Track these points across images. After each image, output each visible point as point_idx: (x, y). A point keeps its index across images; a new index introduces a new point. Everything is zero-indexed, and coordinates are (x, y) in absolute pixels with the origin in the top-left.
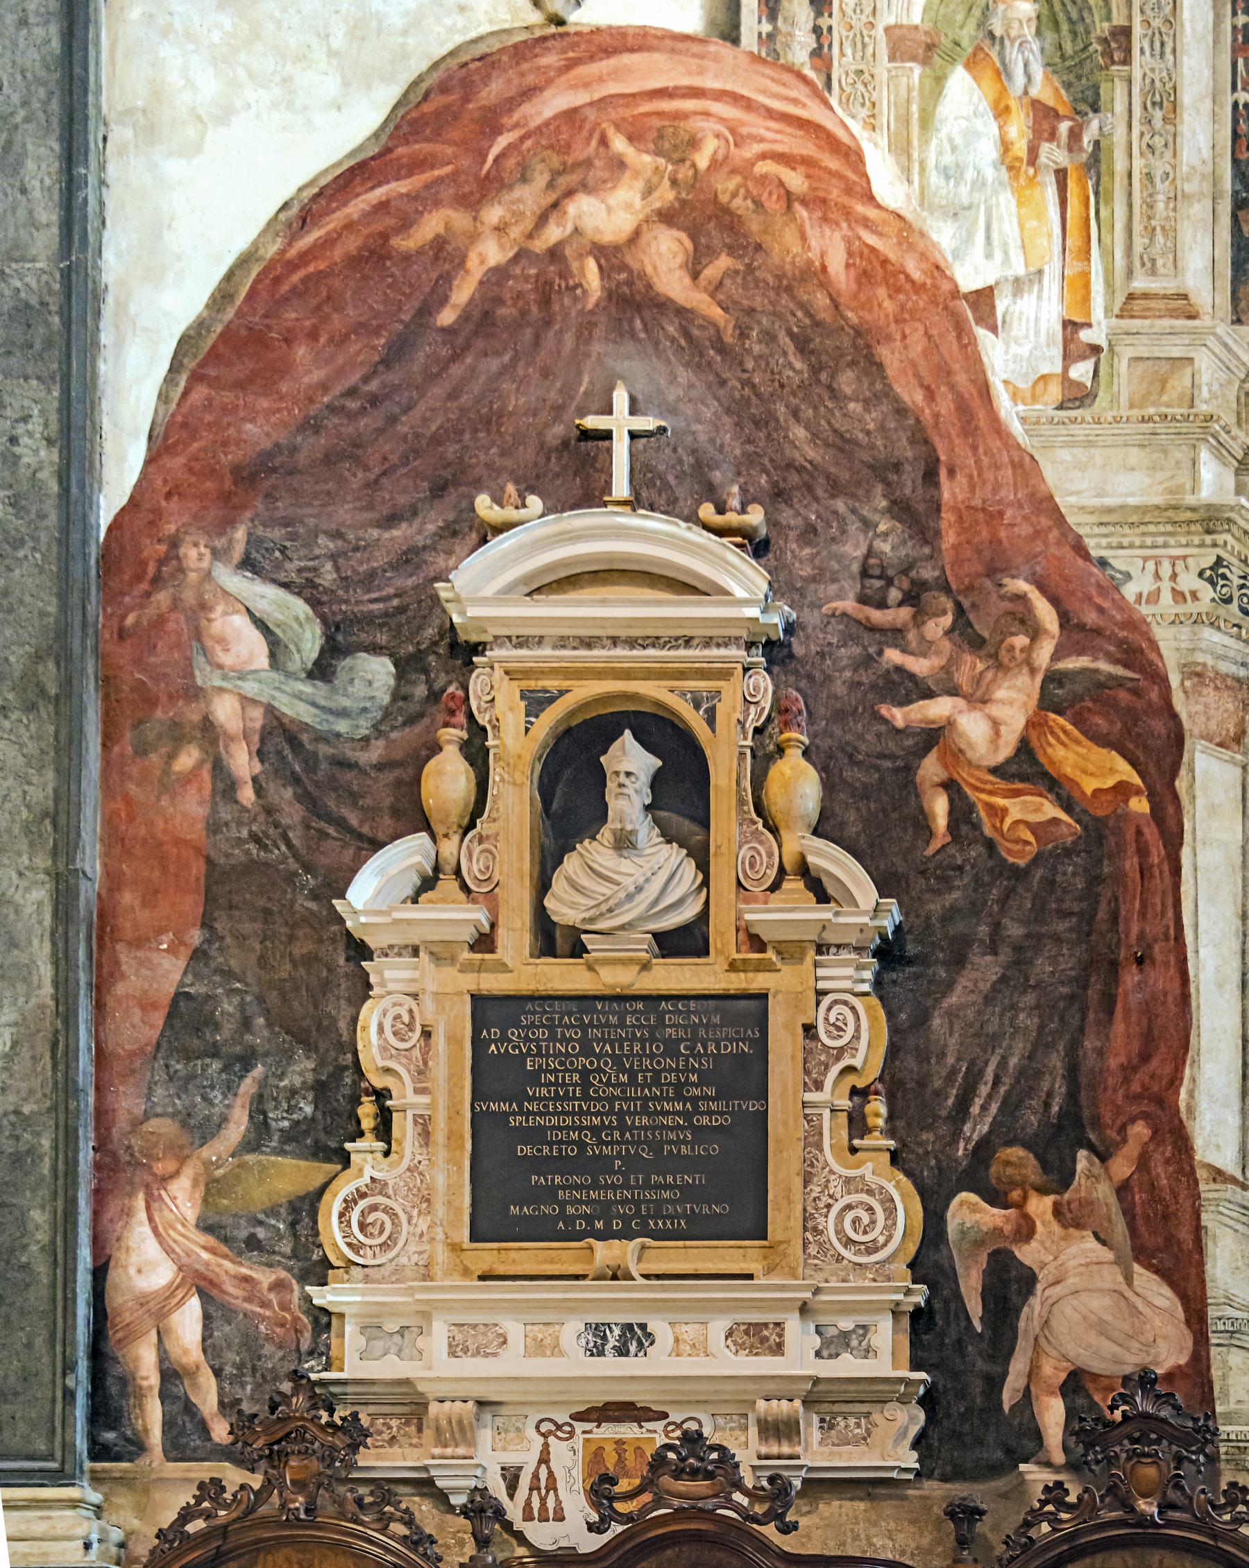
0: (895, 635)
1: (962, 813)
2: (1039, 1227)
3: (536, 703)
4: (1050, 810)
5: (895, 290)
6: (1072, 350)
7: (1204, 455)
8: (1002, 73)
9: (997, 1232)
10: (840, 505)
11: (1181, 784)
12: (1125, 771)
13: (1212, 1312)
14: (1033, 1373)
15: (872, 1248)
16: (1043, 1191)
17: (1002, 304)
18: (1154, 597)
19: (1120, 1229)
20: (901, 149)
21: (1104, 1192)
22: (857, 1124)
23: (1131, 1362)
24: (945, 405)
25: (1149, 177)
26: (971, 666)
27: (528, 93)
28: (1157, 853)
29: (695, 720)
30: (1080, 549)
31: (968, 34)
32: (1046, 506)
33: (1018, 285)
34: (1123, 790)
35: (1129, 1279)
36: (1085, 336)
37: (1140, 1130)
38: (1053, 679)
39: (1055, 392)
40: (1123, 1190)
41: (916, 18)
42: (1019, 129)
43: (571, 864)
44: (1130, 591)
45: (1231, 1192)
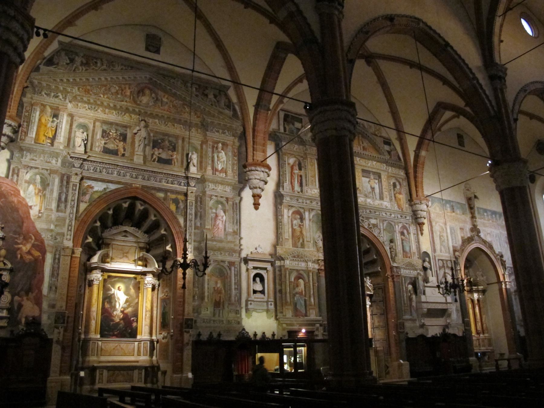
0: (17, 238)
1: (21, 257)
8: (36, 186)
11: (46, 256)
17: (33, 207)
20: (24, 191)
23: (33, 315)
26: (24, 242)
32: (34, 227)
33: (35, 206)
34: (39, 256)
36: (41, 211)
37: (37, 291)
39: (37, 217)
42: (37, 191)
44: (43, 236)
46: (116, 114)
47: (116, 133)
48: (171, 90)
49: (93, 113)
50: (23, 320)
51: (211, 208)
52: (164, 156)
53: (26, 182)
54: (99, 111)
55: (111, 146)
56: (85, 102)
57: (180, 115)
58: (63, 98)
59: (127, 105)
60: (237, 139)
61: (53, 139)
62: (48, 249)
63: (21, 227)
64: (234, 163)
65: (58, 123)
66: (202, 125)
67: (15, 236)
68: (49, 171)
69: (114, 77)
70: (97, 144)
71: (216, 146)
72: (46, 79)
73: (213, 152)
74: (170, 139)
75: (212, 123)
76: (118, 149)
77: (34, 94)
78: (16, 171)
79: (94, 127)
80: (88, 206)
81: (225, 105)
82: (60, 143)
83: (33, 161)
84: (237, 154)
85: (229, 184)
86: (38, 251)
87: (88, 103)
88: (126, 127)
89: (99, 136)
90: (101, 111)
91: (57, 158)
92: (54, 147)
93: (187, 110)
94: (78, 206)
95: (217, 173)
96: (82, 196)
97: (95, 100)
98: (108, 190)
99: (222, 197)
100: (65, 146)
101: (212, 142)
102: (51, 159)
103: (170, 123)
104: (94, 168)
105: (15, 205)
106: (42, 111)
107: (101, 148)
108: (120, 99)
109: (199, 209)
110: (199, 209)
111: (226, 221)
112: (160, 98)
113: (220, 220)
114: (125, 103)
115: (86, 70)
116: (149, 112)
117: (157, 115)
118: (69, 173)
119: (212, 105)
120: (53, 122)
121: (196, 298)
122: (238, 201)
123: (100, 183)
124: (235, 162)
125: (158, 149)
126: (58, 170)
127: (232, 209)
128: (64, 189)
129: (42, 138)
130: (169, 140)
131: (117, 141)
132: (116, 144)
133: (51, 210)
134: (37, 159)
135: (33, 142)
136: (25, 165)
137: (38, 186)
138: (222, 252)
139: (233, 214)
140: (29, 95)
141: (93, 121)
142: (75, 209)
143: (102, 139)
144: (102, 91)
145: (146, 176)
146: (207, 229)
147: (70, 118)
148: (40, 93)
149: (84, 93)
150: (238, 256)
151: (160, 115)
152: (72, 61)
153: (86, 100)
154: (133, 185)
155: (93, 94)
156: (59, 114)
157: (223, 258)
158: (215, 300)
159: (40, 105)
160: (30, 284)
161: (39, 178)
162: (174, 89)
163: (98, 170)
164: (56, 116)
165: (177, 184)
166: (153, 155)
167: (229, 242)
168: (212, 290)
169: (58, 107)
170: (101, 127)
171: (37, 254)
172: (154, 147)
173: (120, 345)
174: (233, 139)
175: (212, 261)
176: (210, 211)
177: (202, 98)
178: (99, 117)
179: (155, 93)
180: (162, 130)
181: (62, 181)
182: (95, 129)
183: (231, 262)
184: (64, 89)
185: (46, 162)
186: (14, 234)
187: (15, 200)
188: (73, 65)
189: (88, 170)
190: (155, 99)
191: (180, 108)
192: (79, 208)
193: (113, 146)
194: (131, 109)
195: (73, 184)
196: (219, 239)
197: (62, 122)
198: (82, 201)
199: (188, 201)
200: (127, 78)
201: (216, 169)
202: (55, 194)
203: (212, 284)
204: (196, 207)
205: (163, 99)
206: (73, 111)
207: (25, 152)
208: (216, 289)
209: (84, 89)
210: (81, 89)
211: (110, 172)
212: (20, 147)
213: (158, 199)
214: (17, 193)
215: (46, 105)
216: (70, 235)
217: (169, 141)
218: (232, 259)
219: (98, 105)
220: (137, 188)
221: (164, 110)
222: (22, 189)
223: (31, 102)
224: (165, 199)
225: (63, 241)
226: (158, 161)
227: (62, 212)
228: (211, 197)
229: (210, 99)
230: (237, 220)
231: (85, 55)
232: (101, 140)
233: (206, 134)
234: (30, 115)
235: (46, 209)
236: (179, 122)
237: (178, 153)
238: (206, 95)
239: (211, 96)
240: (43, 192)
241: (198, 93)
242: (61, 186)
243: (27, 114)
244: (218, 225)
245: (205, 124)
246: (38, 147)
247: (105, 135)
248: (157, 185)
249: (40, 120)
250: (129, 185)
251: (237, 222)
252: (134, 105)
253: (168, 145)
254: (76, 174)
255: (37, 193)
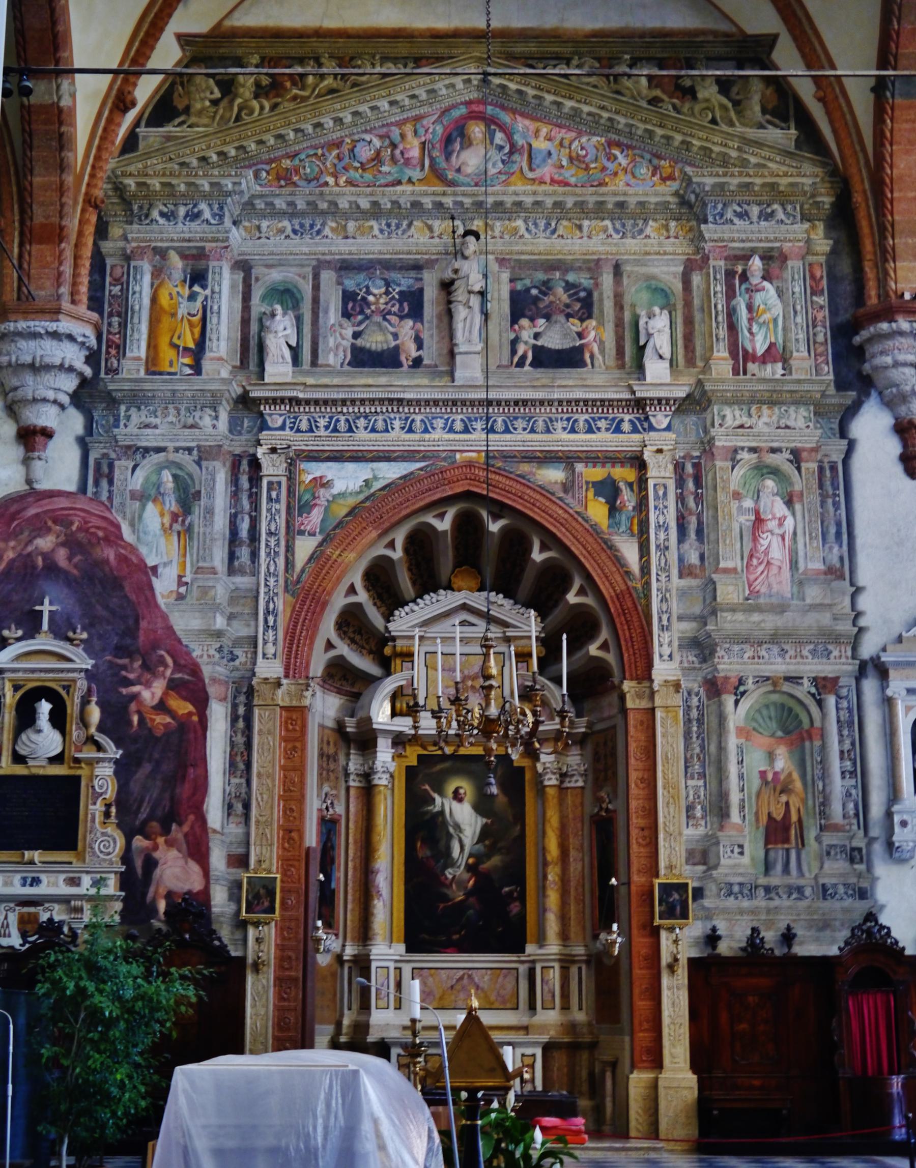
0: (124, 668)
1: (142, 720)
2: (160, 847)
3: (16, 688)
4: (168, 720)
5: (128, 566)
6: (181, 583)
7: (218, 615)
8: (163, 503)
9: (147, 848)
10: (109, 628)
11: (208, 712)
12: (190, 708)
13: (212, 873)
14: (156, 892)
15: (109, 854)
16: (162, 835)
17: (160, 570)
18: (202, 656)
19: (184, 847)
20: (132, 525)
21: (180, 836)
22: (107, 815)
24: (142, 600)
25: (204, 534)
27: (24, 509)
28: (200, 733)
29: (63, 693)
30: (179, 641)
31: (153, 492)
32: (170, 629)
33: (165, 565)
34: (190, 714)
35: (186, 863)
36: (184, 579)
37: (191, 817)
38: (171, 680)
39: (174, 596)
40: (186, 835)
41: (138, 488)
42: (167, 520)
43: (24, 737)
44: (194, 654)
45: (218, 836)
46: (381, 231)
47: (387, 293)
48: (559, 104)
49: (308, 245)
50: (162, 906)
51: (737, 496)
52: (554, 340)
53: (134, 496)
54: (327, 231)
55: (375, 341)
56: (282, 214)
57: (600, 185)
58: (214, 215)
59: (413, 193)
60: (820, 227)
61: (198, 352)
62: (212, 690)
63: (132, 632)
64: (814, 320)
65: (206, 298)
66: (684, 202)
67: (121, 661)
68: (195, 452)
69: (364, 108)
70: (331, 342)
71: (740, 269)
72: (160, 167)
73: (730, 294)
74: (571, 277)
75: (721, 188)
76: (397, 348)
77: (131, 223)
78: (105, 469)
79: (316, 287)
80: (320, 544)
81: (764, 111)
82: (220, 359)
83: (149, 431)
84: (824, 282)
85: (798, 401)
86: (185, 699)
87: (292, 213)
88: (417, 267)
89: (332, 314)
90: (333, 230)
91: (215, 410)
92: (204, 376)
93: (622, 160)
94: (290, 549)
95: (751, 366)
96: (300, 515)
97: (311, 198)
98: (377, 485)
99: (773, 450)
100: (234, 367)
101: (726, 259)
102: (198, 414)
103: (565, 223)
104: (330, 423)
105: (111, 570)
106: (157, 273)
107: (345, 351)
108: (390, 179)
109: (691, 503)
110: (691, 503)
111: (795, 533)
112: (520, 141)
113: (771, 532)
114: (409, 188)
115: (274, 107)
116: (490, 200)
117: (519, 204)
118: (251, 451)
119: (714, 121)
120: (192, 297)
121: (698, 812)
122: (837, 457)
123: (350, 466)
124: (820, 316)
125: (532, 320)
126: (220, 446)
127: (816, 486)
128: (246, 504)
129: (167, 354)
130: (567, 282)
131: (394, 319)
132: (391, 329)
133: (213, 571)
134: (158, 421)
135: (142, 373)
136: (129, 447)
137: (168, 505)
138: (786, 647)
139: (823, 504)
140: (115, 231)
141: (310, 269)
142: (281, 561)
143: (345, 321)
144: (328, 164)
145: (500, 420)
146: (726, 571)
147: (242, 275)
148: (147, 216)
149: (275, 183)
150: (849, 653)
151: (528, 200)
152: (228, 86)
153: (284, 206)
154: (458, 456)
155: (301, 183)
156: (207, 270)
157: (792, 667)
158: (769, 815)
159: (150, 253)
160: (172, 799)
161: (171, 479)
162: (571, 98)
163: (342, 425)
164: (198, 277)
165: (607, 430)
166: (514, 343)
167: (815, 607)
168: (756, 782)
169: (203, 248)
170: (339, 283)
171: (183, 707)
172: (514, 320)
173: (470, 976)
174: (807, 232)
175: (750, 681)
176: (735, 505)
177: (675, 107)
178: (331, 253)
179: (503, 128)
180: (540, 254)
181: (234, 480)
182: (321, 295)
183: (825, 678)
184: (212, 184)
185: (185, 427)
186: (116, 656)
187: (110, 554)
188: (231, 102)
189: (311, 430)
190: (507, 150)
191: (596, 160)
192: (293, 555)
193: (380, 338)
194: (427, 202)
195: (270, 484)
196: (774, 600)
197: (220, 293)
198: (301, 533)
199: (651, 483)
200: (407, 102)
201: (745, 352)
202: (221, 523)
203: (756, 761)
204: (681, 498)
205: (536, 144)
206: (248, 250)
207: (123, 408)
208: (770, 777)
209: (273, 173)
210: (264, 174)
211: (380, 425)
212: (109, 393)
213: (544, 491)
214: (113, 536)
215: (168, 248)
216: (274, 644)
217: (569, 286)
218: (826, 669)
219: (323, 213)
220: (470, 464)
221: (542, 182)
222: (124, 518)
223: (124, 249)
224: (567, 487)
225: (254, 664)
226: (536, 364)
227: (242, 572)
228: (733, 454)
229: (707, 100)
230: (839, 524)
231: (263, 59)
232: (341, 326)
233: (701, 232)
234: (125, 290)
235: (198, 570)
236: (599, 211)
237: (601, 323)
238: (690, 93)
239: (709, 92)
240: (183, 521)
241: (658, 93)
242: (235, 495)
243: (116, 290)
244: (766, 552)
245: (693, 197)
246: (156, 385)
247: (353, 308)
248: (538, 442)
249: (154, 300)
250: (445, 459)
251: (838, 534)
252: (440, 189)
253: (565, 298)
254: (273, 450)
255: (167, 525)
